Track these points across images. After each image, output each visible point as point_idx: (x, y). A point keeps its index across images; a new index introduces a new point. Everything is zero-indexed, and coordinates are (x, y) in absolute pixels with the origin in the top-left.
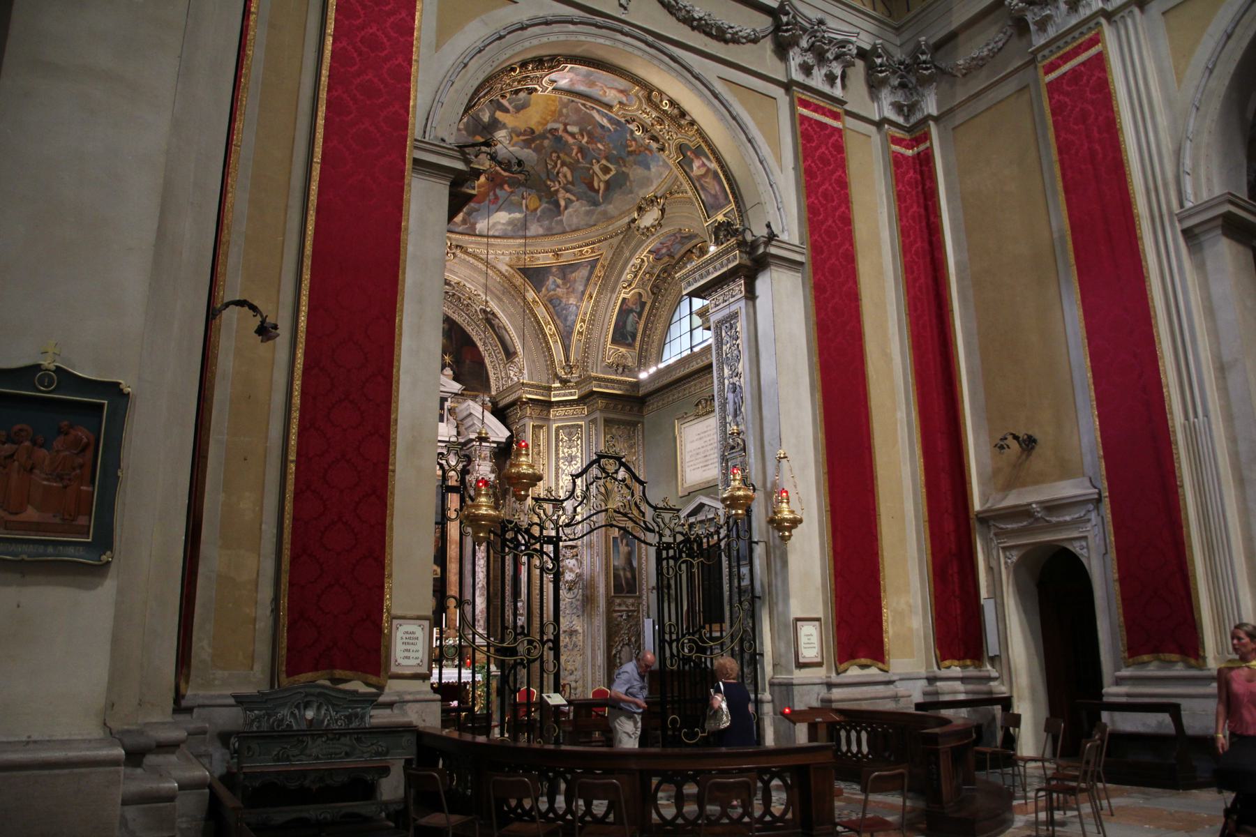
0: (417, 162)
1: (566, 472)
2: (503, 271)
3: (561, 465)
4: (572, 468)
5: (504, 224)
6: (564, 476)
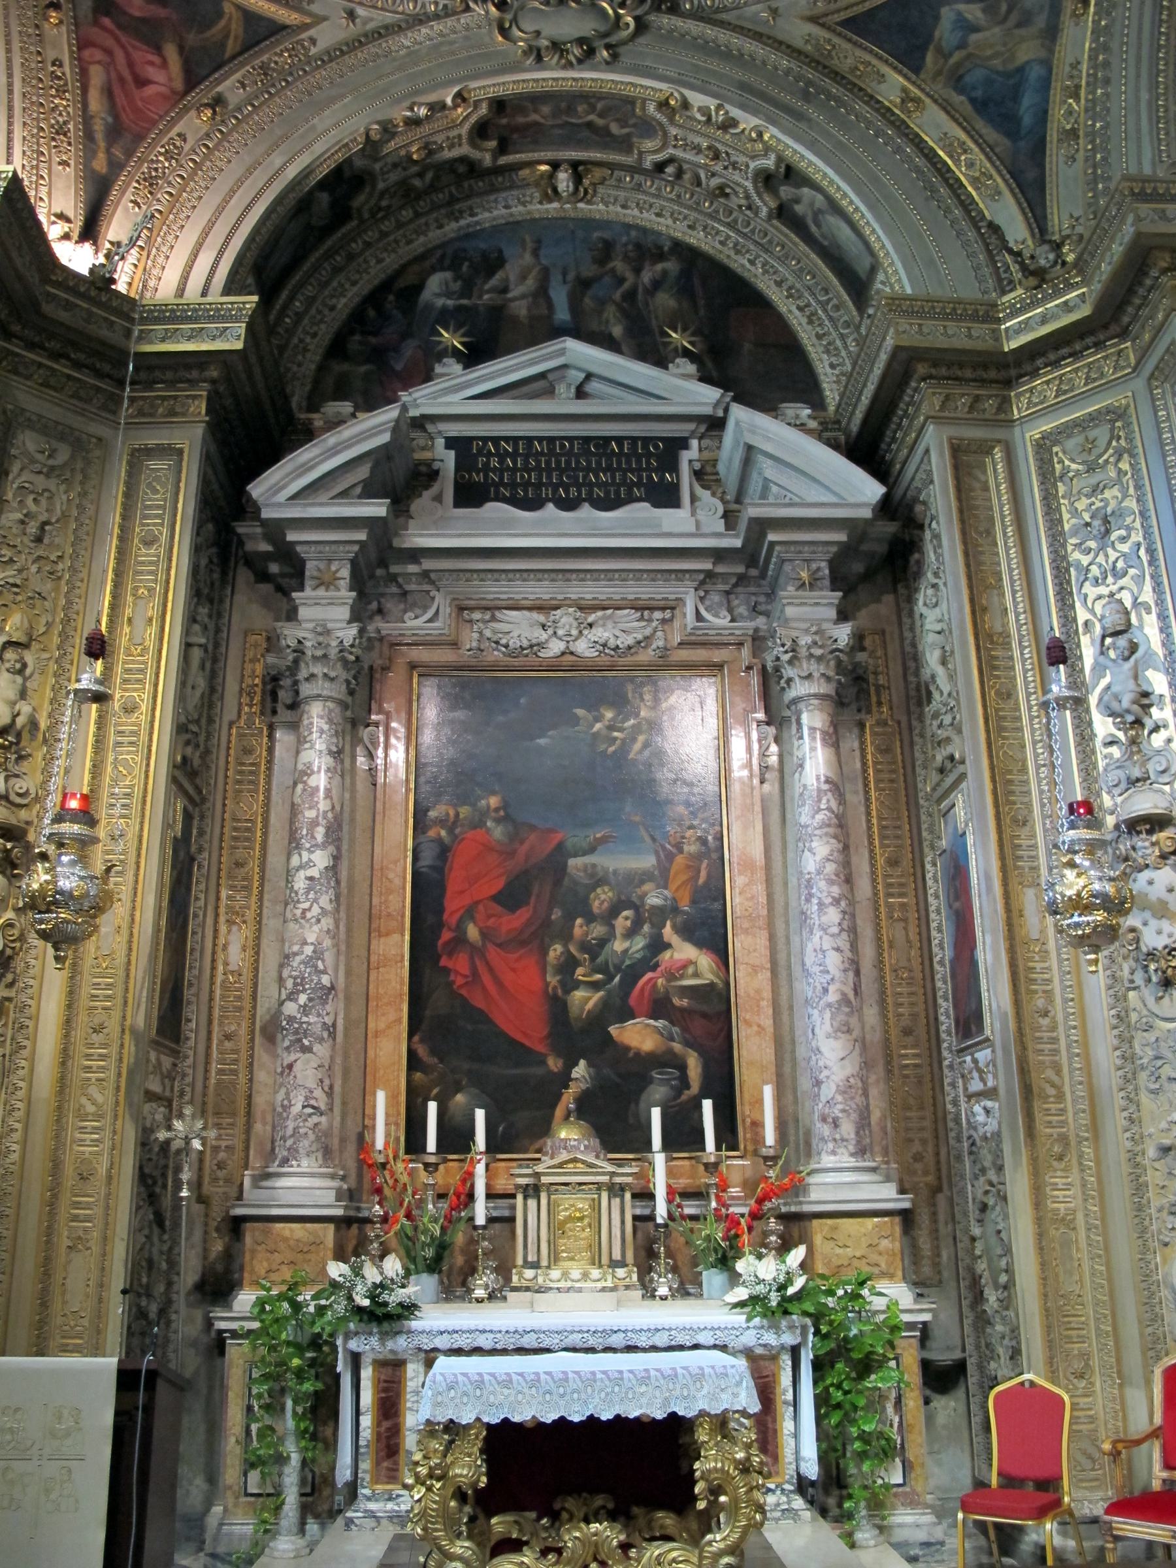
1: (1095, 571)
2: (798, 43)
3: (1076, 556)
4: (1113, 555)
6: (1088, 588)
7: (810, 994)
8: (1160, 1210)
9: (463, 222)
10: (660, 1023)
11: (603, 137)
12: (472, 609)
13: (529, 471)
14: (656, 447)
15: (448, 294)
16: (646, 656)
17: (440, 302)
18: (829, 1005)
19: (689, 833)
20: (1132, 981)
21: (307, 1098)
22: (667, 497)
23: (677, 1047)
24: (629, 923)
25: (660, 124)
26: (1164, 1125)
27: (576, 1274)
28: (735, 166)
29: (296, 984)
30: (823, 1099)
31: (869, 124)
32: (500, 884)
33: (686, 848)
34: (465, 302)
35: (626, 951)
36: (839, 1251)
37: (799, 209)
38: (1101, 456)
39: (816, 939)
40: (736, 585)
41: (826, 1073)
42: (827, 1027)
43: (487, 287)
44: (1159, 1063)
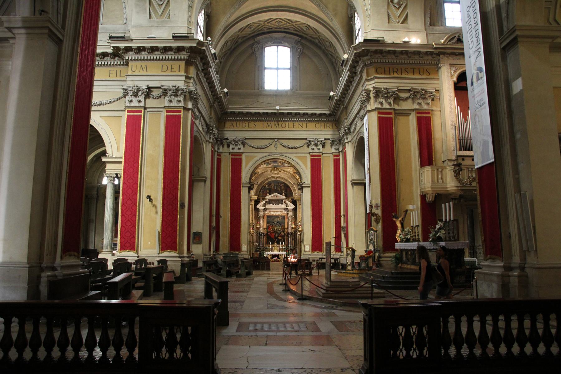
0: (243, 186)
22: (282, 204)
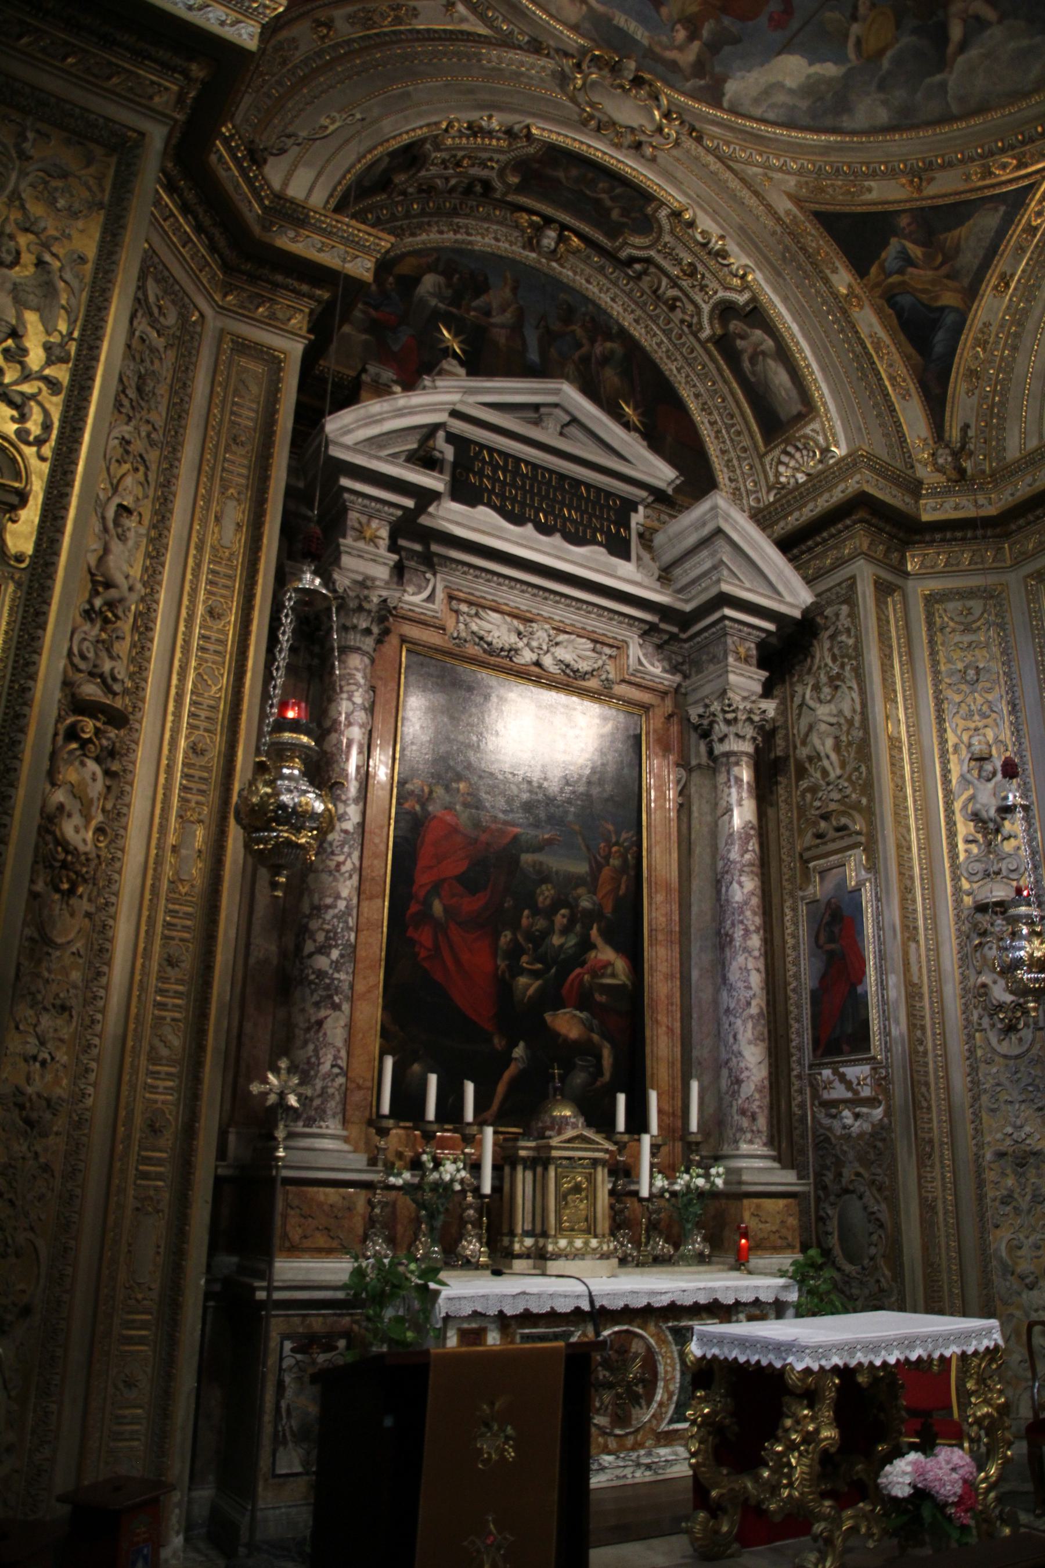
3: (949, 693)
5: (791, 91)
7: (732, 1006)
8: (994, 1200)
9: (459, 237)
10: (583, 1015)
11: (599, 216)
12: (460, 600)
13: (517, 489)
14: (615, 503)
15: (441, 298)
16: (593, 683)
17: (433, 302)
18: (751, 1017)
19: (614, 849)
20: (980, 1024)
21: (336, 1058)
22: (620, 549)
23: (596, 1037)
24: (565, 921)
25: (660, 228)
26: (999, 1136)
27: (579, 1243)
28: (703, 288)
29: (327, 938)
30: (743, 1096)
31: (825, 302)
32: (462, 867)
33: (611, 861)
34: (454, 310)
35: (562, 946)
36: (761, 1226)
37: (740, 343)
38: (975, 621)
39: (741, 959)
40: (666, 642)
41: (746, 1074)
42: (749, 1034)
43: (474, 304)
44: (999, 1089)
